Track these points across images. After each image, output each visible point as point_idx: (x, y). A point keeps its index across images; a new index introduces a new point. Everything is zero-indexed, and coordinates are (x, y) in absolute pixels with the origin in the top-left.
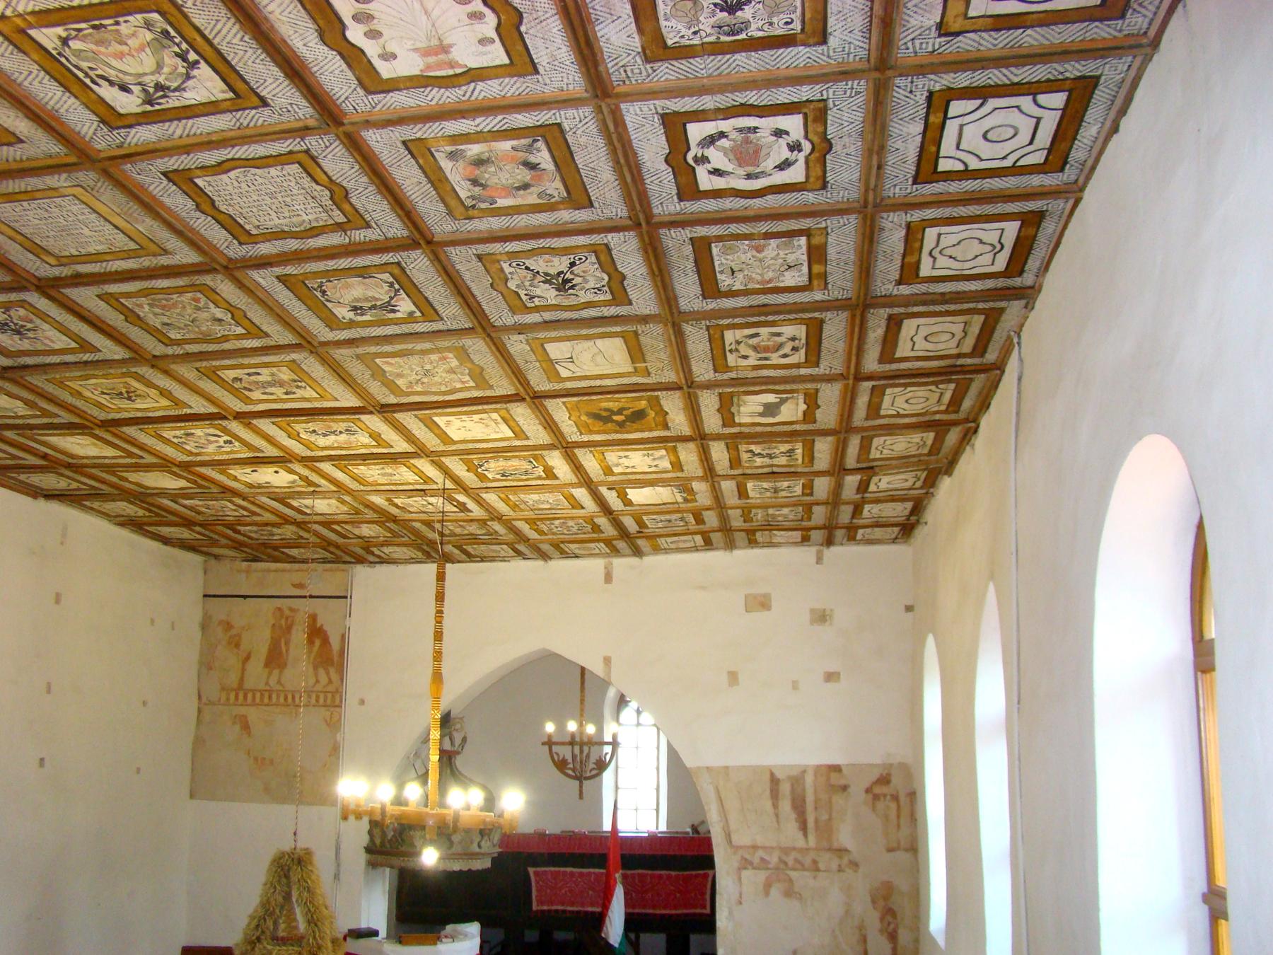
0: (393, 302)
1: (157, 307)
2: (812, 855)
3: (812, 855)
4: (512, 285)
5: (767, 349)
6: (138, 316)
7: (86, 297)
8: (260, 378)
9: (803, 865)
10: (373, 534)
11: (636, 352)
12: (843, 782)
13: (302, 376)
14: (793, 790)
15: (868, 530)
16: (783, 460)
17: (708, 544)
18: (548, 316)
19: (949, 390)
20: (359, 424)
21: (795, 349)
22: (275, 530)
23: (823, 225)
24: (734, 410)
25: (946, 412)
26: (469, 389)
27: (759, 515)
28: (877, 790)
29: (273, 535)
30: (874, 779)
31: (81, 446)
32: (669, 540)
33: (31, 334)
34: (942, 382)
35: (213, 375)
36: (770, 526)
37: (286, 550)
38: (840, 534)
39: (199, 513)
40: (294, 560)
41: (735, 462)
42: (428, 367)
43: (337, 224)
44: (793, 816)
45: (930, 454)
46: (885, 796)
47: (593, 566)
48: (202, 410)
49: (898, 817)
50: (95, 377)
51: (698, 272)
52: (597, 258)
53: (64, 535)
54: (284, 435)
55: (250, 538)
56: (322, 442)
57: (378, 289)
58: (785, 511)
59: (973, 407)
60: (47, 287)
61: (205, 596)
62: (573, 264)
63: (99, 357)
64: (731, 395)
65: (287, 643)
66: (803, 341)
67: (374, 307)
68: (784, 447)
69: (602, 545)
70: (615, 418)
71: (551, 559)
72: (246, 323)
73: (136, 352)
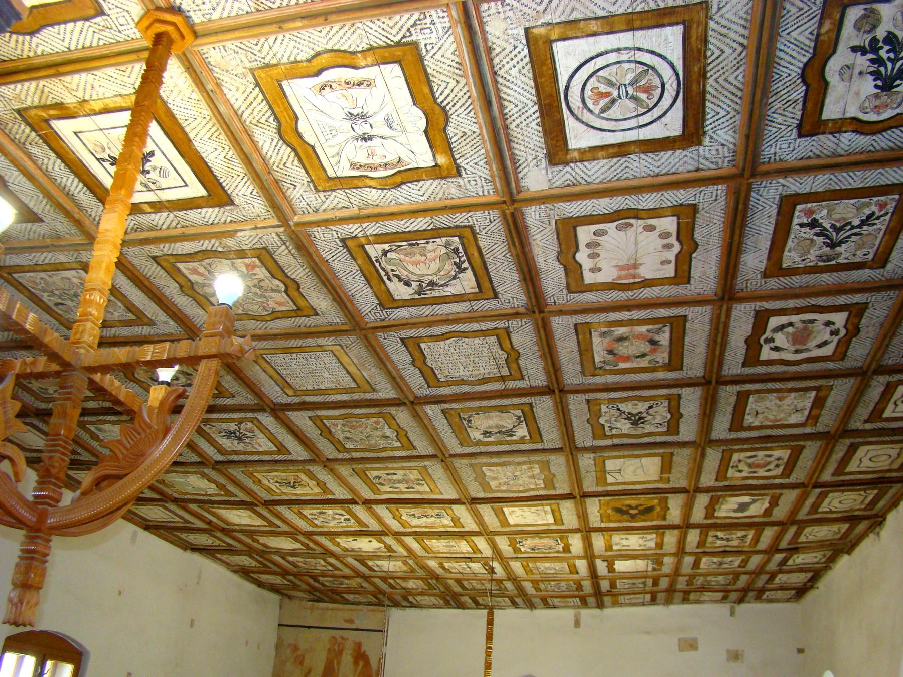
0: (514, 430)
1: (348, 426)
4: (602, 421)
5: (759, 466)
6: (330, 432)
7: (301, 419)
8: (395, 477)
10: (415, 587)
11: (666, 467)
13: (426, 476)
15: (772, 593)
16: (735, 543)
17: (653, 601)
18: (616, 441)
19: (872, 494)
20: (450, 512)
21: (777, 466)
22: (346, 581)
23: (831, 383)
24: (717, 507)
25: (864, 509)
26: (538, 489)
27: (699, 581)
29: (341, 584)
31: (239, 517)
32: (627, 597)
33: (247, 441)
34: (870, 489)
35: (363, 476)
36: (702, 589)
37: (345, 596)
38: (751, 594)
39: (296, 566)
40: (347, 602)
41: (702, 543)
42: (517, 474)
43: (502, 376)
45: (840, 539)
47: (567, 615)
48: (341, 497)
50: (277, 471)
51: (733, 415)
52: (669, 404)
53: (199, 577)
54: (391, 515)
55: (324, 585)
56: (415, 521)
57: (507, 421)
58: (720, 578)
59: (885, 506)
60: (278, 410)
61: (279, 625)
62: (650, 407)
63: (289, 457)
64: (720, 497)
65: (339, 663)
66: (785, 461)
67: (499, 432)
68: (740, 534)
69: (578, 600)
70: (631, 511)
71: (535, 608)
72: (404, 440)
73: (317, 456)
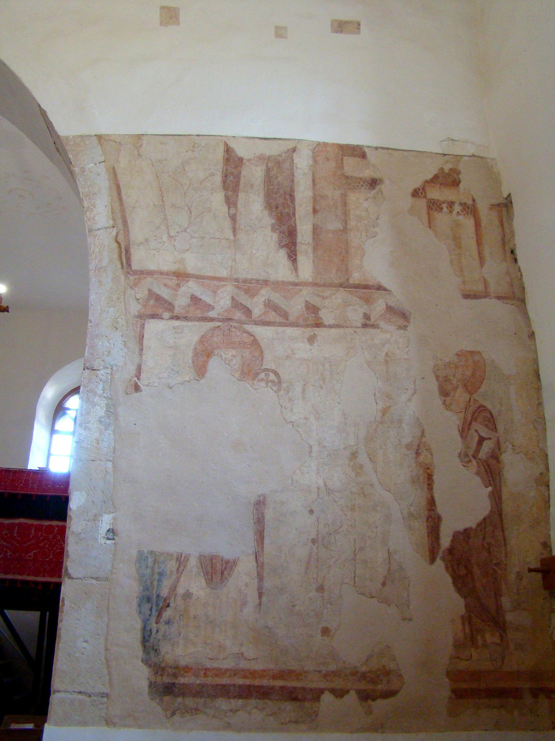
2: (306, 294)
3: (306, 294)
9: (285, 315)
12: (367, 173)
14: (269, 179)
28: (434, 194)
30: (429, 176)
44: (268, 220)
46: (451, 204)
49: (479, 243)
